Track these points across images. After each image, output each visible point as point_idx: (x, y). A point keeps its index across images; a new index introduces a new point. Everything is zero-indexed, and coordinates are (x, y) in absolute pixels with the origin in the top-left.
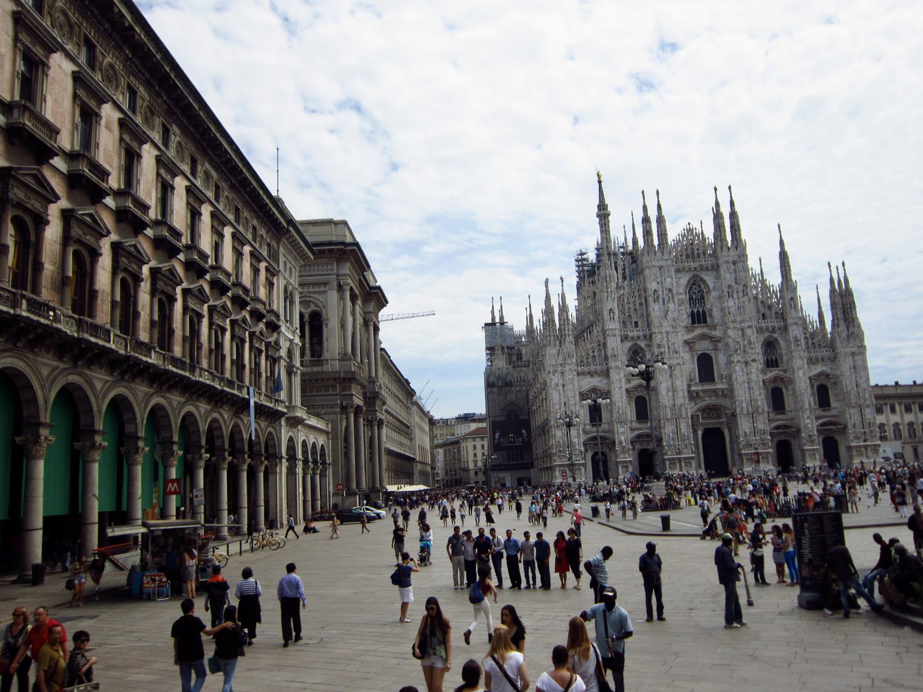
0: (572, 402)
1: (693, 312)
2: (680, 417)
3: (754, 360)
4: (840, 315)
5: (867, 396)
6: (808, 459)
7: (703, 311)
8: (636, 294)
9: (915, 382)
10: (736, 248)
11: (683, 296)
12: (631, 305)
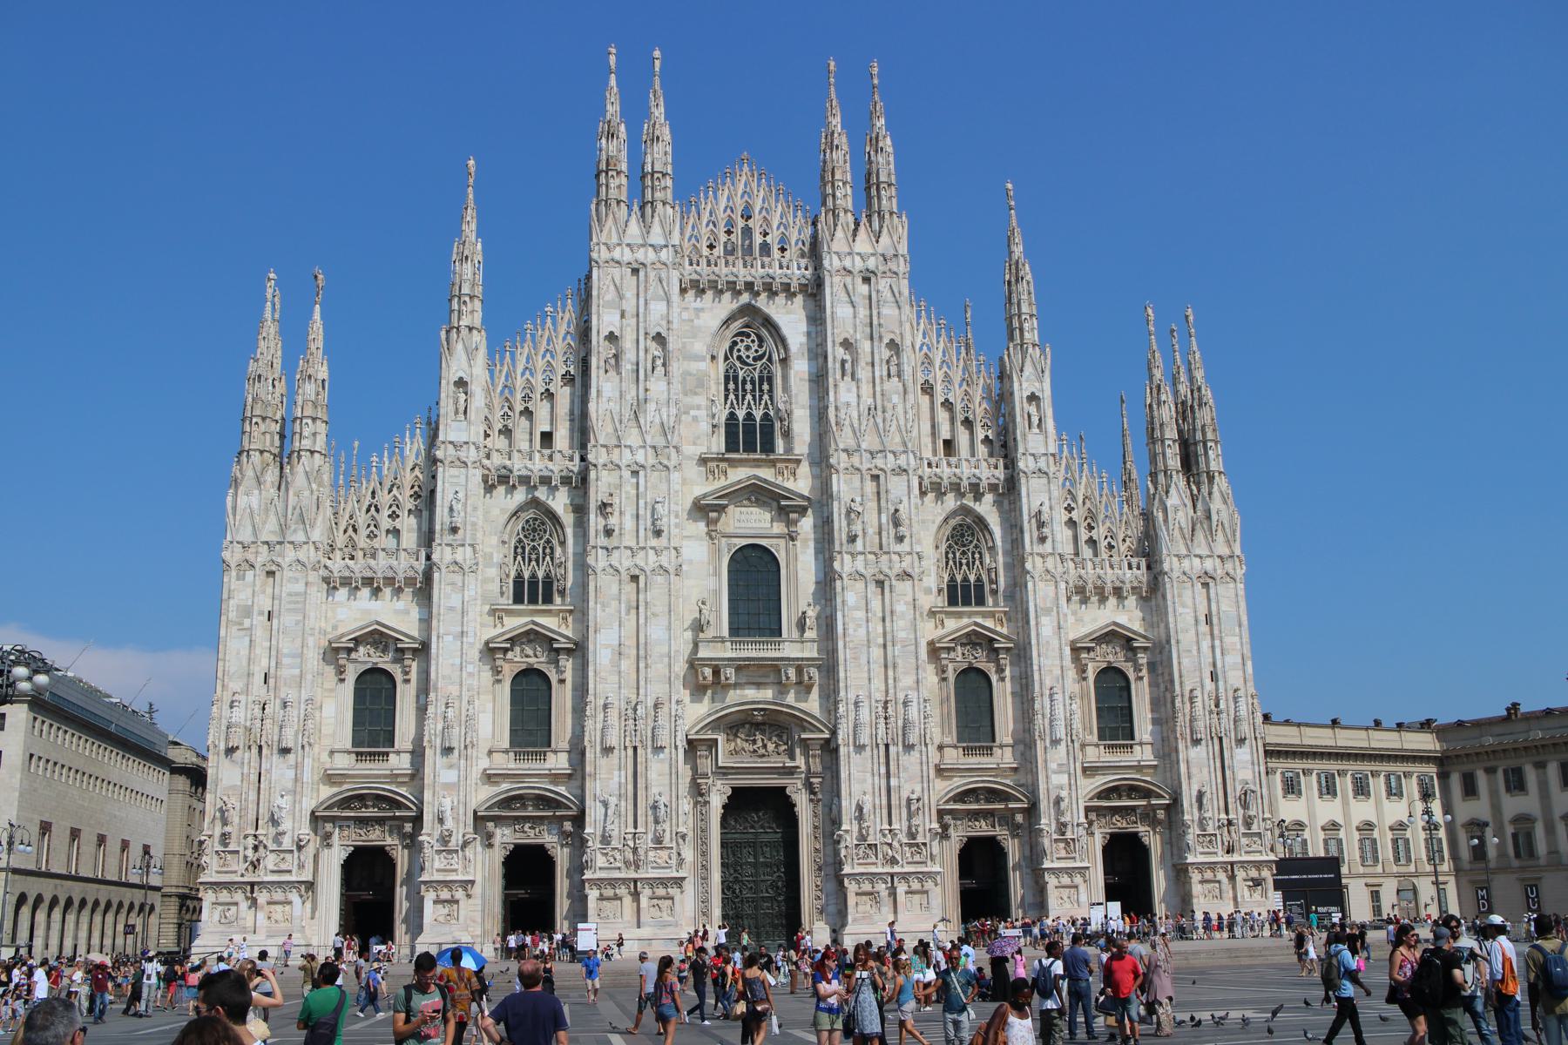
0: (288, 671)
1: (732, 416)
3: (906, 575)
4: (1174, 462)
7: (766, 415)
8: (560, 346)
9: (1377, 723)
11: (704, 365)
12: (540, 377)
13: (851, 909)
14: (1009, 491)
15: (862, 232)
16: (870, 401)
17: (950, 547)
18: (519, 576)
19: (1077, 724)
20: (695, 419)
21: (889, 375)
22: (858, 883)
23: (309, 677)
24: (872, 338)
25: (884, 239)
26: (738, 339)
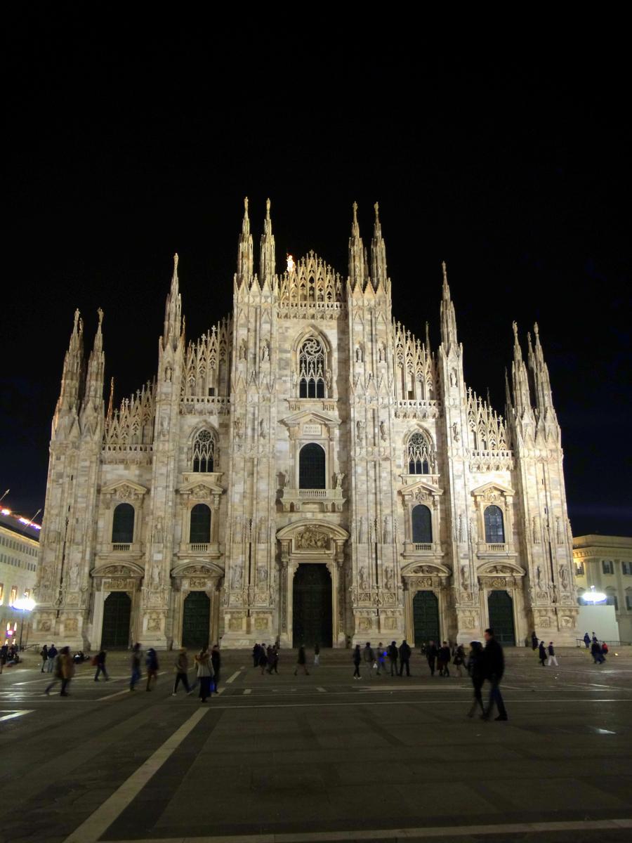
0: (81, 505)
2: (258, 540)
3: (387, 459)
5: (562, 529)
6: (460, 625)
7: (320, 380)
10: (376, 289)
12: (209, 361)
13: (357, 627)
14: (442, 415)
15: (369, 287)
16: (371, 372)
17: (411, 445)
18: (197, 459)
19: (474, 535)
20: (285, 382)
21: (380, 359)
22: (360, 612)
23: (91, 508)
24: (372, 341)
25: (380, 291)
26: (307, 342)
